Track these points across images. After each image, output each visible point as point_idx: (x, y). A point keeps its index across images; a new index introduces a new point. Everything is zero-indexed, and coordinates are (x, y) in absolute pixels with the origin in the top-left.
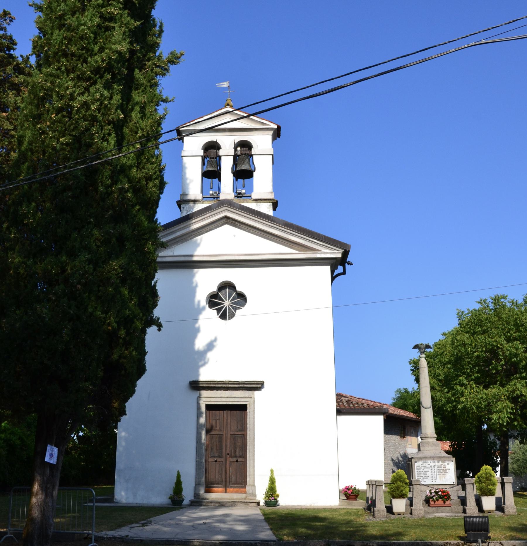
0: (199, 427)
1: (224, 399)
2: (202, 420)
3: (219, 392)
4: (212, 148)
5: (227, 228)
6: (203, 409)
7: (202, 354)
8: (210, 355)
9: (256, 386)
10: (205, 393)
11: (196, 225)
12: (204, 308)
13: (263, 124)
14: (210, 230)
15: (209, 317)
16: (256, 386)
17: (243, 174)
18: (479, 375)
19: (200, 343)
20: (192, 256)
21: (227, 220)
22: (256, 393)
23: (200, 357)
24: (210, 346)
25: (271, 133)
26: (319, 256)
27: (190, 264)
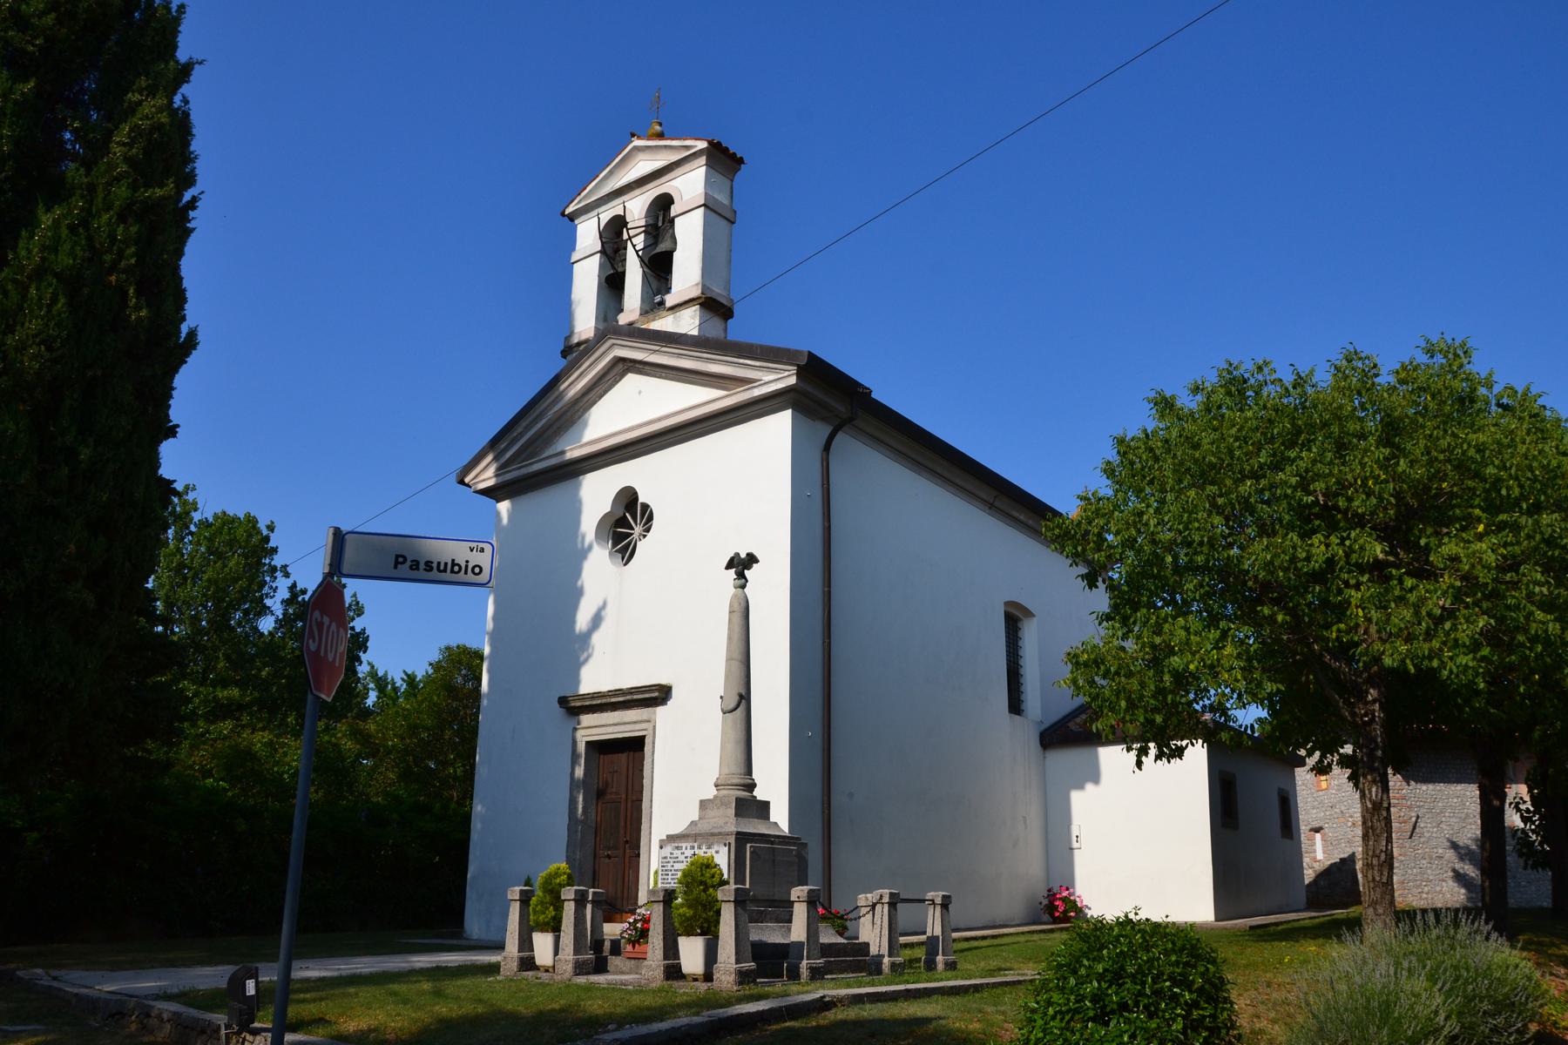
0: (573, 782)
1: (610, 729)
2: (580, 772)
3: (605, 715)
4: (614, 232)
5: (632, 381)
6: (582, 748)
7: (586, 638)
8: (596, 638)
9: (660, 695)
10: (587, 719)
11: (574, 386)
12: (590, 547)
13: (687, 148)
14: (606, 392)
15: (599, 565)
16: (660, 695)
17: (659, 266)
18: (266, 625)
19: (582, 620)
20: (563, 452)
21: (625, 366)
22: (660, 710)
23: (576, 648)
24: (597, 620)
25: (703, 160)
26: (757, 392)
27: (575, 469)
